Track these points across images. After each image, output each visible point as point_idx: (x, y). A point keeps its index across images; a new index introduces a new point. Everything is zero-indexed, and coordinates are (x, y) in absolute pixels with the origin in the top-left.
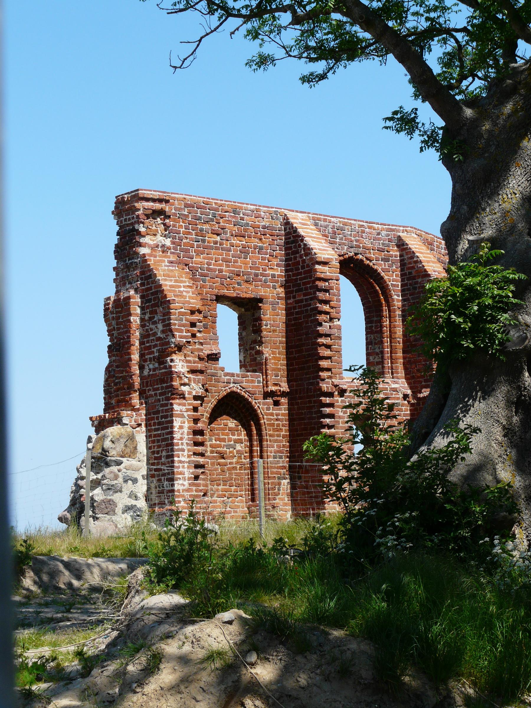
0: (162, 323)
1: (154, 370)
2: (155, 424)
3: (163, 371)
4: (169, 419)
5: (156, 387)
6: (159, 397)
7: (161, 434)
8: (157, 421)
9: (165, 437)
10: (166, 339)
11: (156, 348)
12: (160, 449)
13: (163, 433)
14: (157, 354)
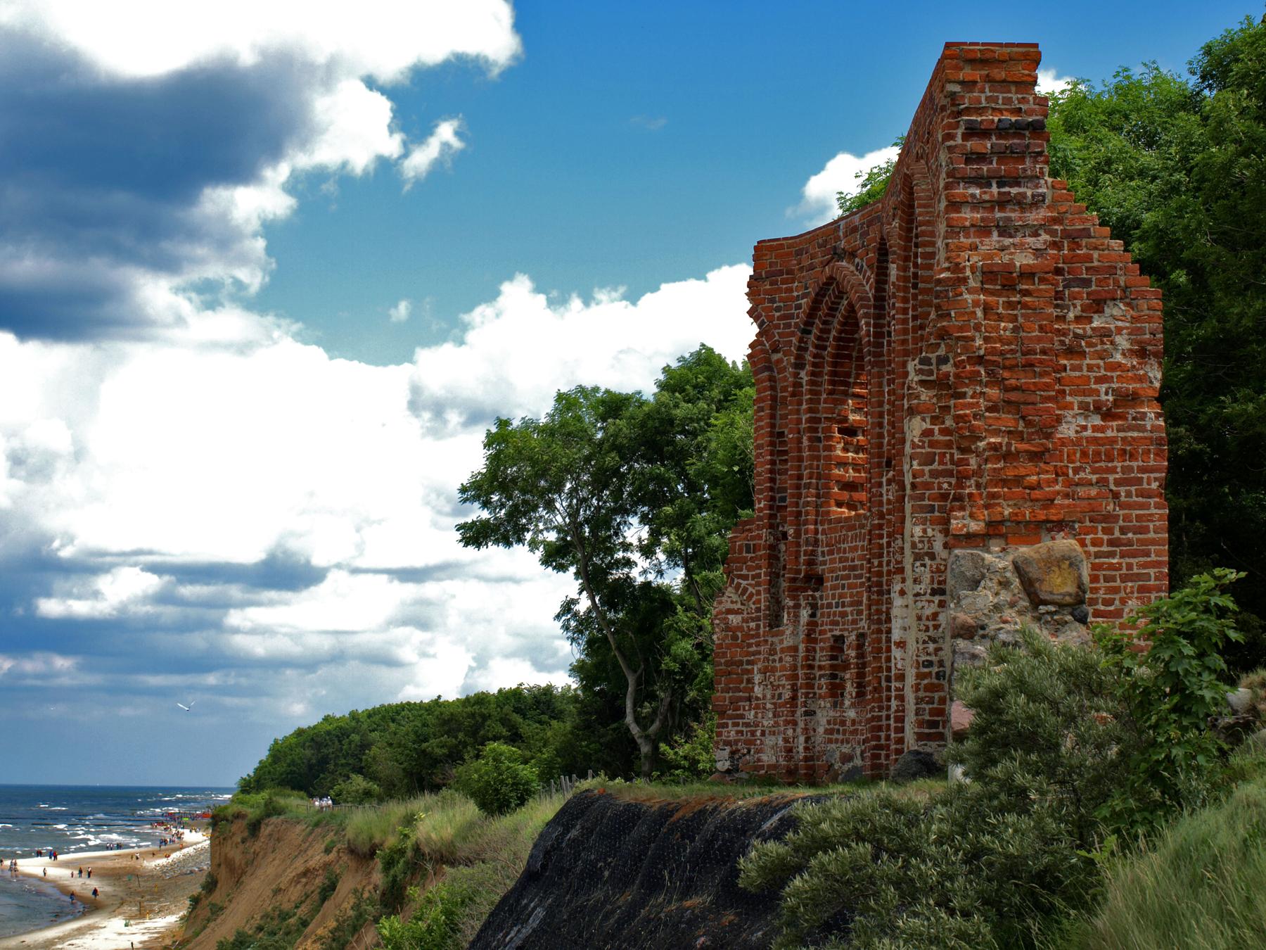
0: (1129, 334)
1: (1095, 428)
2: (1094, 544)
3: (1135, 434)
4: (1152, 535)
5: (1103, 464)
6: (1114, 488)
7: (1120, 564)
8: (1105, 537)
9: (1135, 571)
10: (1138, 370)
11: (1106, 385)
12: (1117, 597)
13: (1130, 567)
14: (1111, 398)
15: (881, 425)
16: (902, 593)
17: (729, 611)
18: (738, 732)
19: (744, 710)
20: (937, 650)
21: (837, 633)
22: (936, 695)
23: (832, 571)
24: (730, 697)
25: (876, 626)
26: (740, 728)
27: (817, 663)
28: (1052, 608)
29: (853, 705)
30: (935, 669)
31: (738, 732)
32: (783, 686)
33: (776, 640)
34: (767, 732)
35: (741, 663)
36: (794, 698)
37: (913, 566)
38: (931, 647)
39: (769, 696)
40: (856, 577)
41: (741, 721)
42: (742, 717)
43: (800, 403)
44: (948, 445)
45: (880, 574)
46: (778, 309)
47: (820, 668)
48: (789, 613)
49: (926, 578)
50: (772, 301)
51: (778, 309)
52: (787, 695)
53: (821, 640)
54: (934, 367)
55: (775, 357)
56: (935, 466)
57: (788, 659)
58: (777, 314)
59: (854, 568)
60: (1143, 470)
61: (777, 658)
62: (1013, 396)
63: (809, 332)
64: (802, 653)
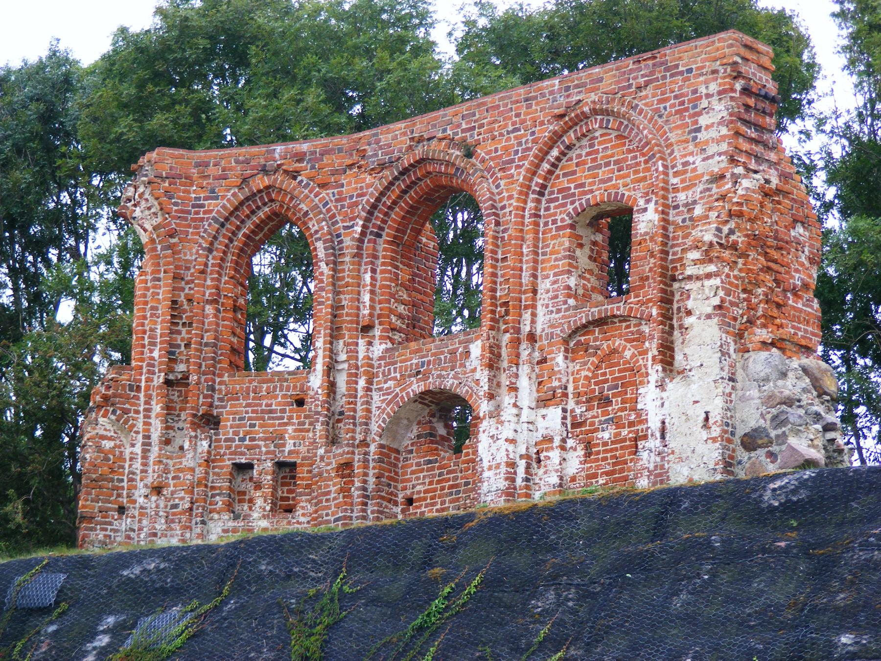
3: (810, 310)
15: (358, 300)
16: (515, 405)
17: (103, 437)
18: (105, 536)
19: (113, 518)
20: (732, 417)
21: (243, 461)
22: (731, 446)
23: (228, 413)
24: (100, 507)
25: (351, 449)
26: (108, 533)
27: (210, 484)
28: (828, 398)
29: (264, 517)
30: (730, 429)
31: (105, 536)
32: (182, 499)
33: (171, 462)
34: (159, 535)
35: (112, 480)
36: (191, 509)
37: (720, 358)
38: (729, 414)
39: (162, 505)
40: (269, 418)
41: (109, 527)
42: (110, 524)
43: (205, 281)
44: (737, 286)
45: (355, 411)
46: (176, 204)
47: (213, 488)
48: (190, 441)
49: (726, 368)
50: (170, 198)
51: (176, 204)
52: (187, 506)
53: (214, 468)
54: (723, 235)
55: (173, 241)
56: (731, 298)
57: (189, 477)
58: (176, 208)
59: (271, 412)
60: (813, 334)
61: (170, 476)
62: (771, 264)
63: (223, 225)
64: (199, 472)
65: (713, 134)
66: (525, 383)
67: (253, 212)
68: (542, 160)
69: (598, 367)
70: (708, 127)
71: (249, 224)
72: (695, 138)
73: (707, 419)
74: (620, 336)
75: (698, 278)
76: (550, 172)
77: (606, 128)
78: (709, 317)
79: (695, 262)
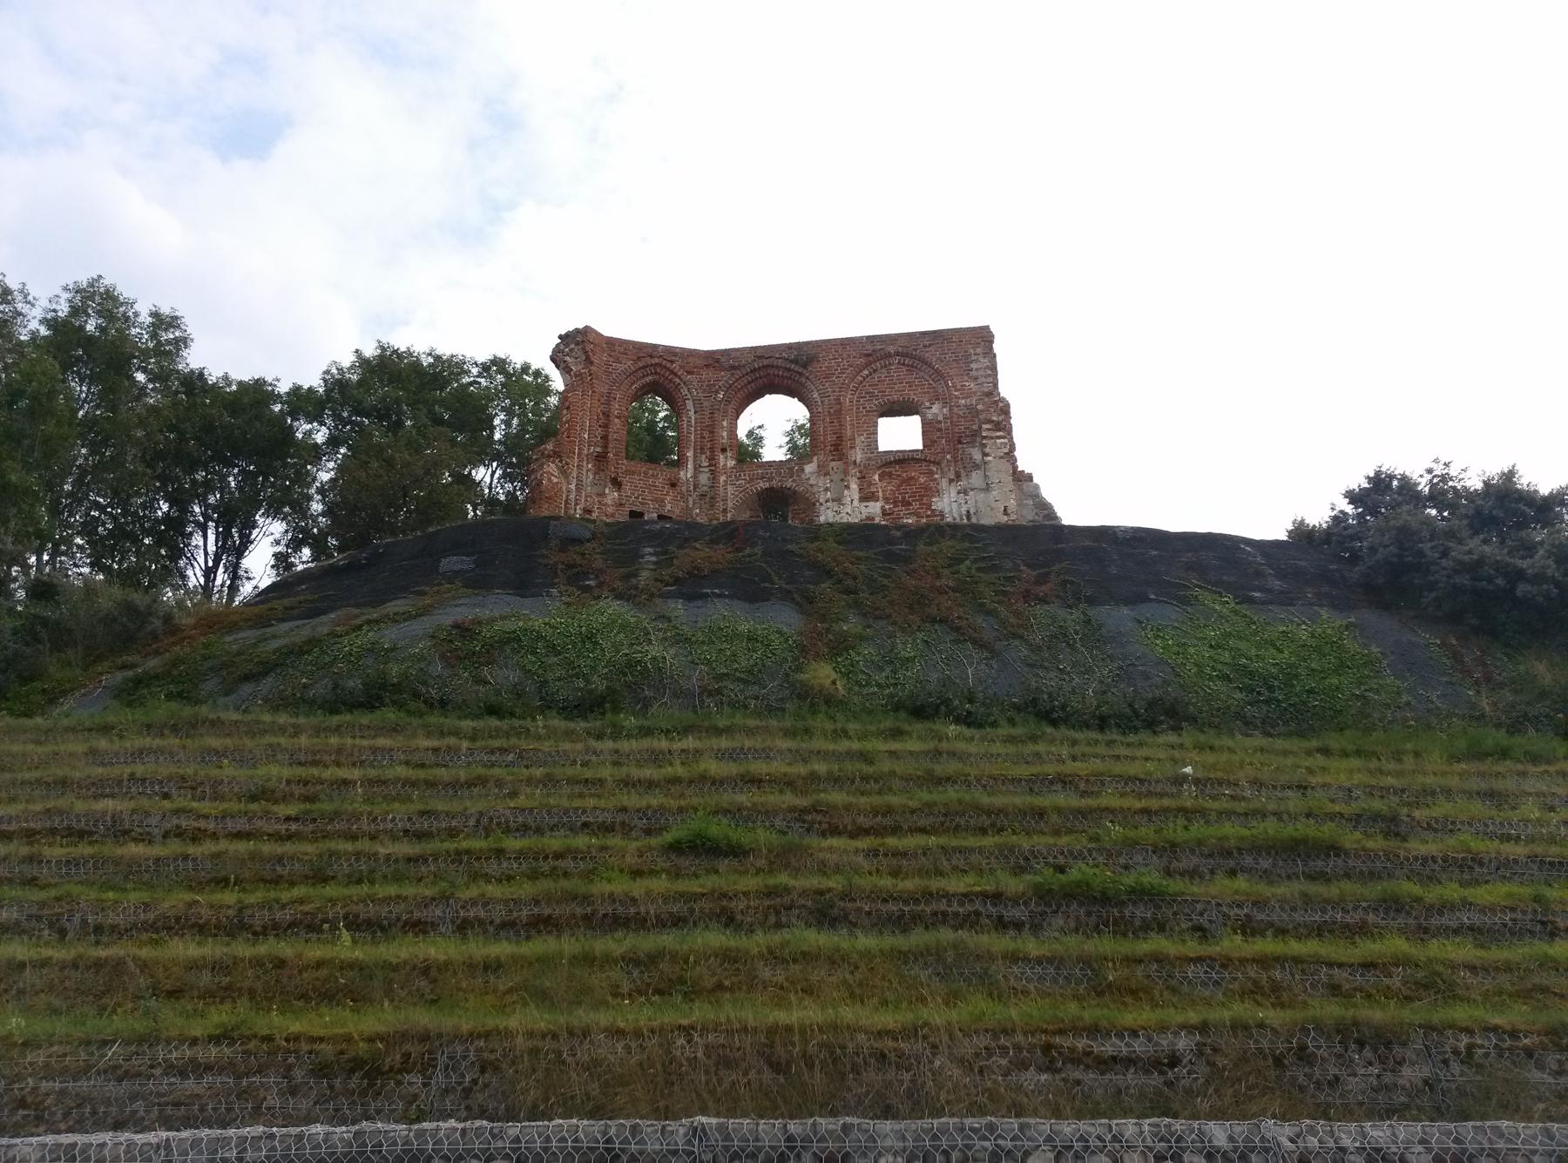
65: (981, 373)
66: (854, 486)
67: (643, 377)
68: (858, 374)
69: (899, 486)
70: (977, 369)
71: (639, 383)
72: (968, 374)
73: (1005, 510)
74: (915, 471)
75: (992, 438)
76: (861, 382)
77: (904, 364)
78: (1001, 458)
79: (989, 430)
